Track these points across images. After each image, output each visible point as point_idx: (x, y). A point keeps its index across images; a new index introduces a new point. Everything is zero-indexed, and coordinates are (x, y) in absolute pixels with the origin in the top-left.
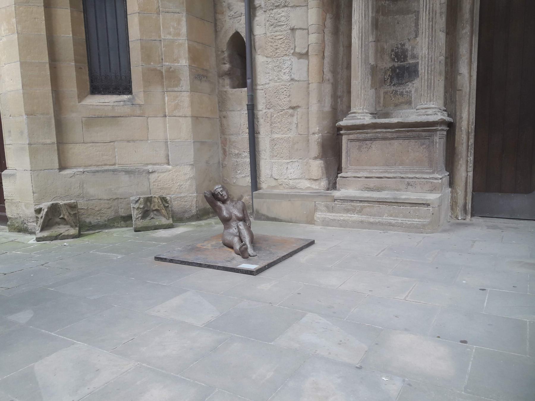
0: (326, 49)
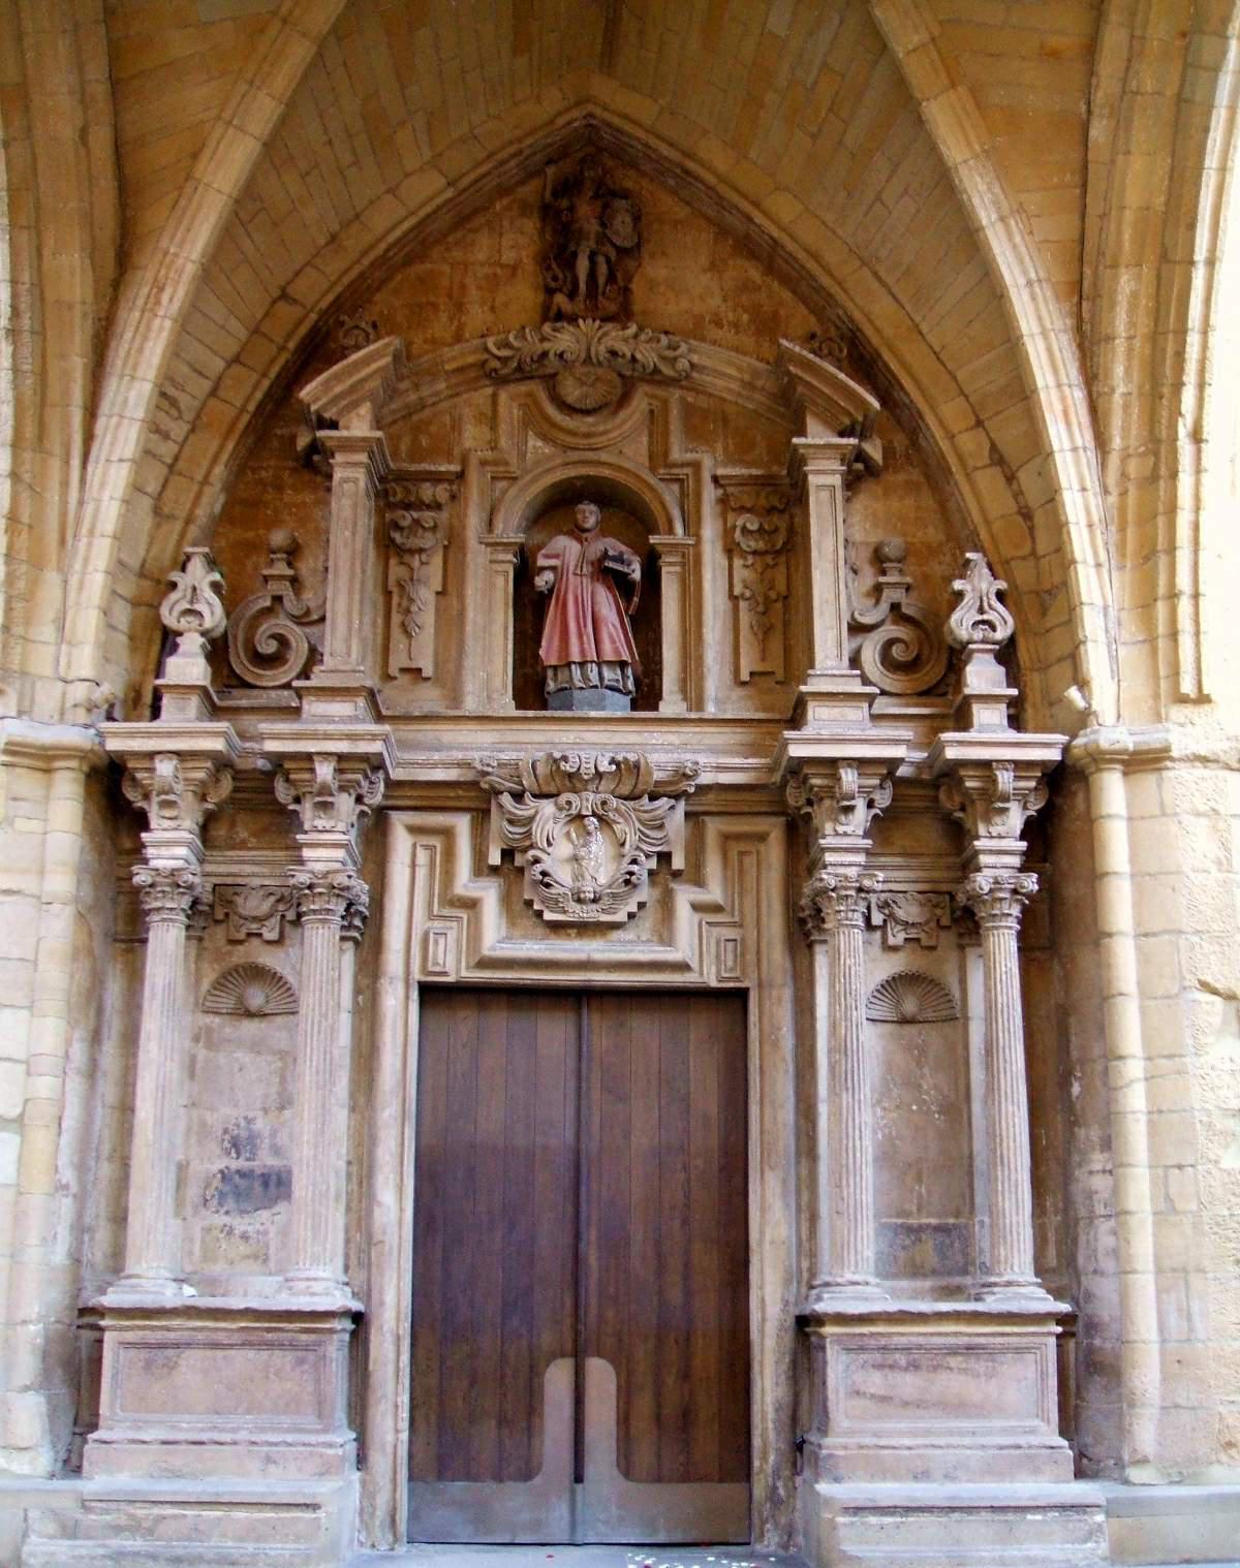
0: (67, 1113)
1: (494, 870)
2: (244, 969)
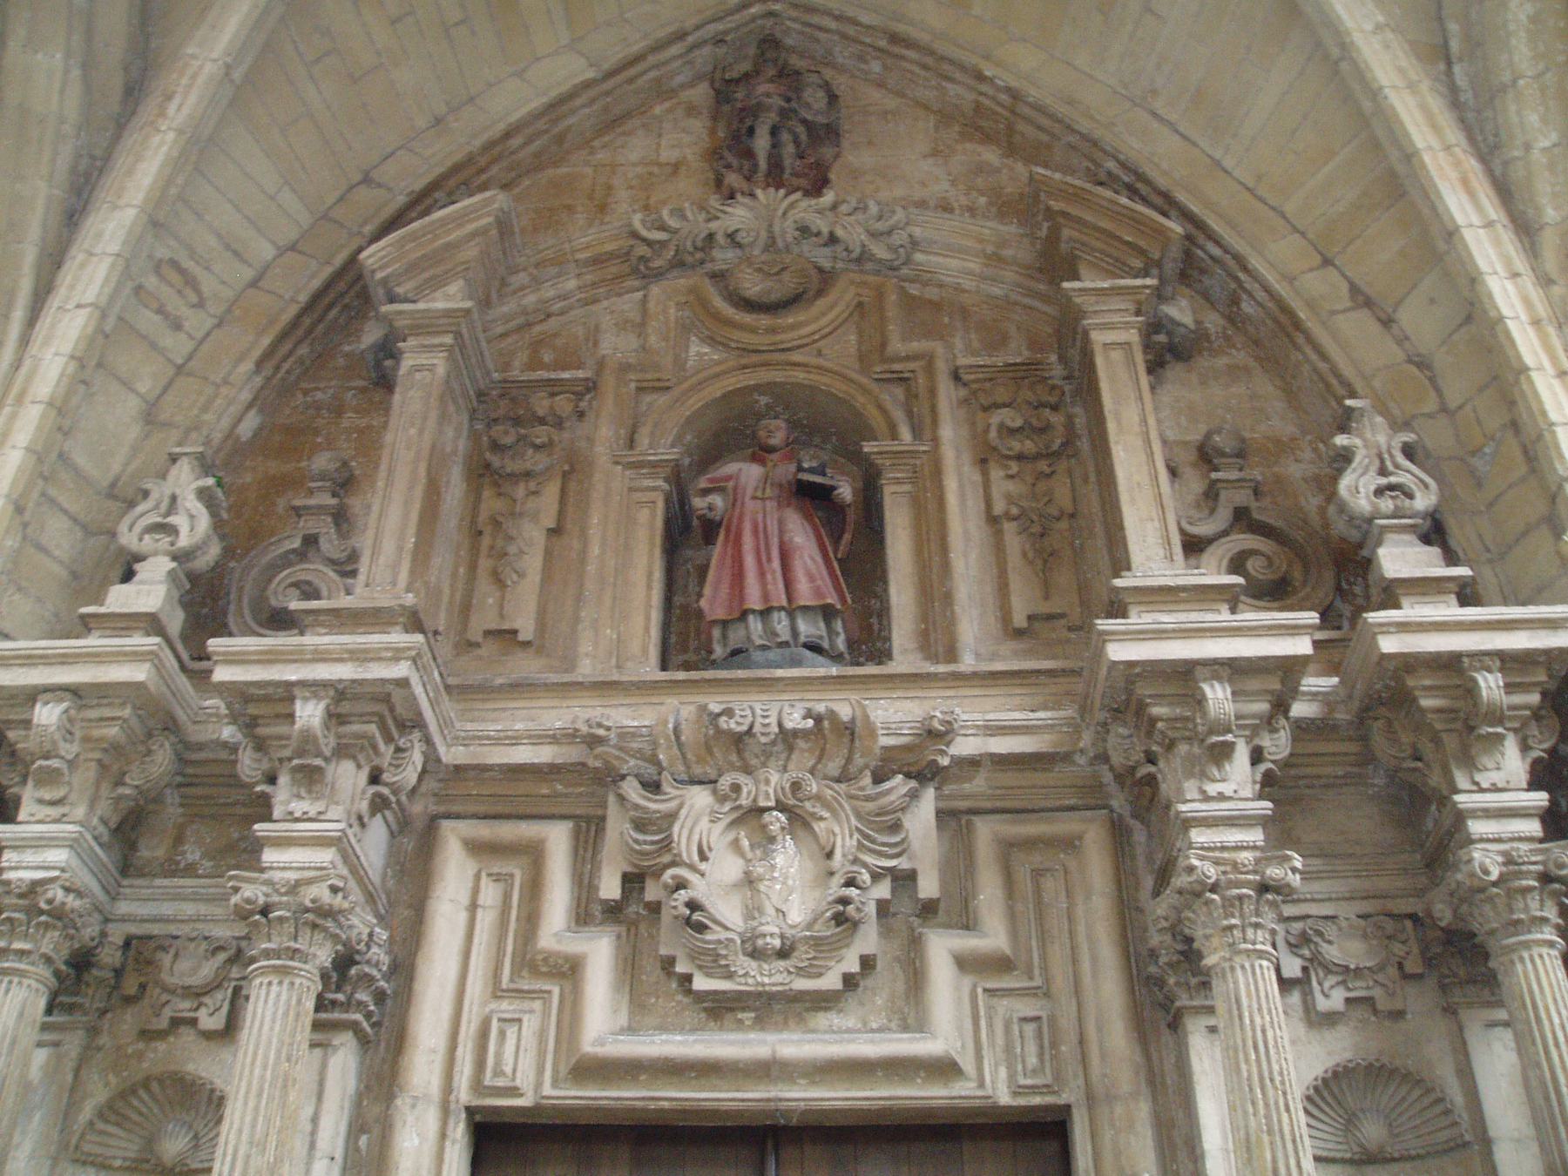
1: (613, 911)
2: (161, 1081)
